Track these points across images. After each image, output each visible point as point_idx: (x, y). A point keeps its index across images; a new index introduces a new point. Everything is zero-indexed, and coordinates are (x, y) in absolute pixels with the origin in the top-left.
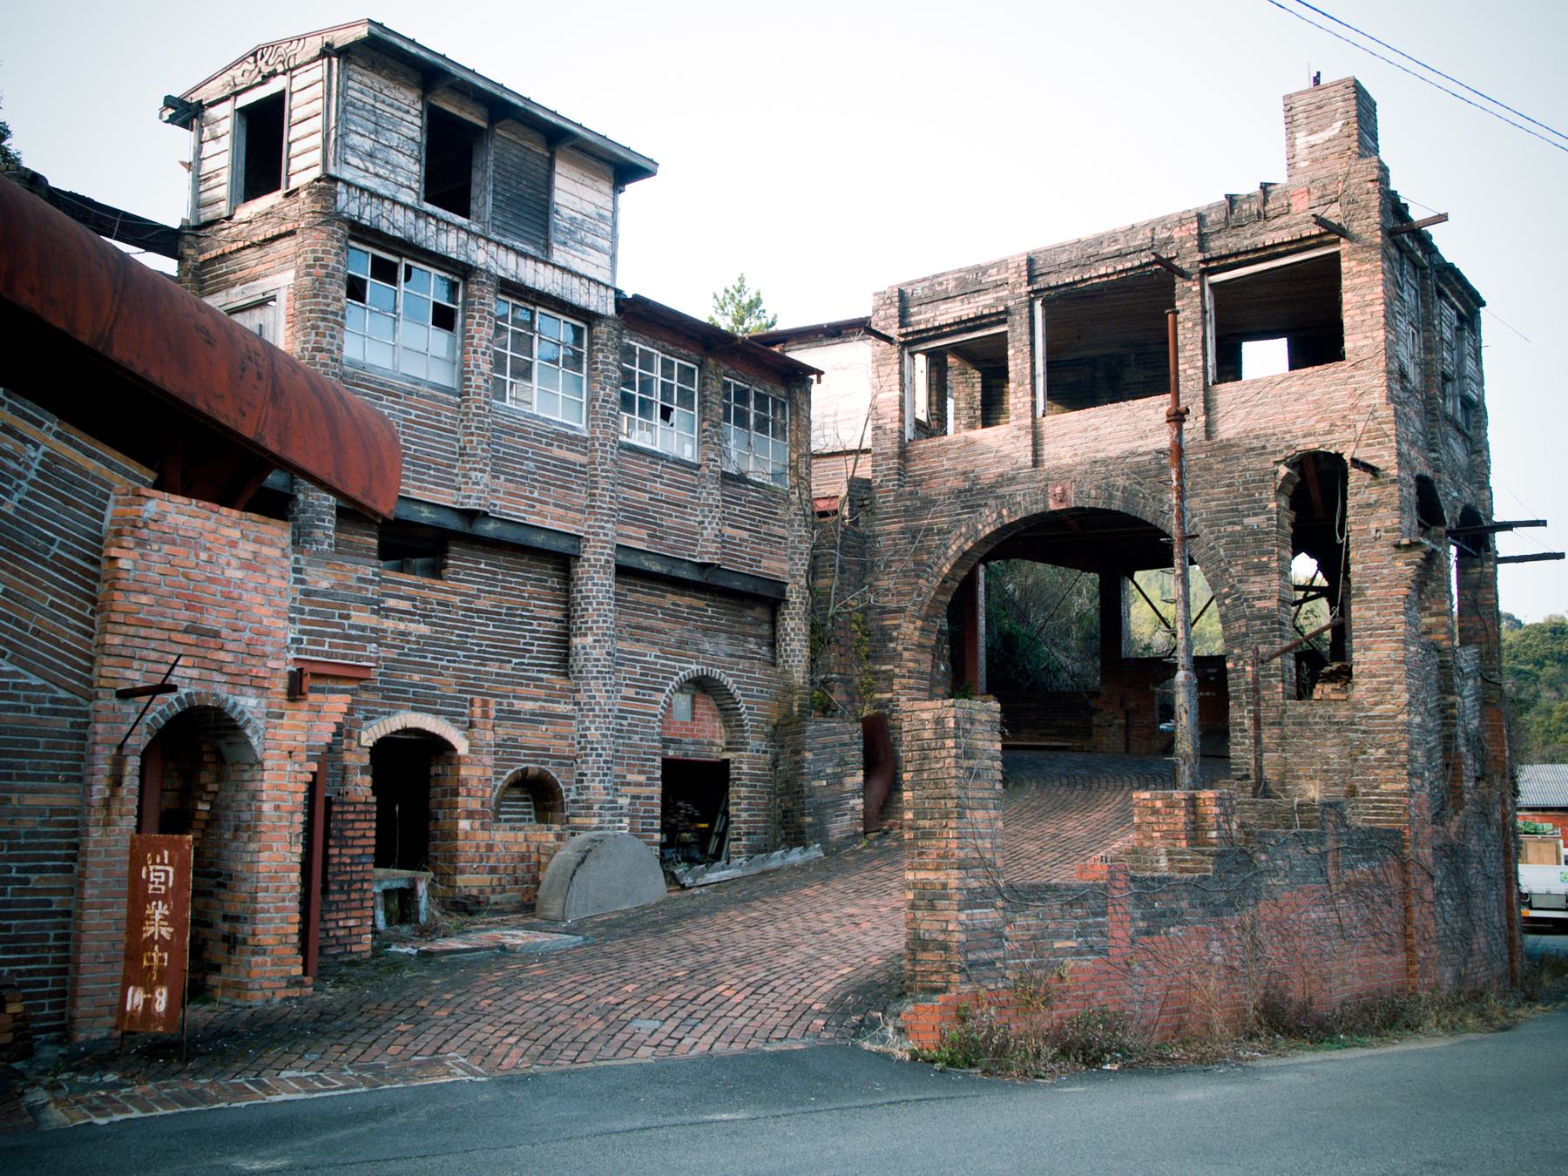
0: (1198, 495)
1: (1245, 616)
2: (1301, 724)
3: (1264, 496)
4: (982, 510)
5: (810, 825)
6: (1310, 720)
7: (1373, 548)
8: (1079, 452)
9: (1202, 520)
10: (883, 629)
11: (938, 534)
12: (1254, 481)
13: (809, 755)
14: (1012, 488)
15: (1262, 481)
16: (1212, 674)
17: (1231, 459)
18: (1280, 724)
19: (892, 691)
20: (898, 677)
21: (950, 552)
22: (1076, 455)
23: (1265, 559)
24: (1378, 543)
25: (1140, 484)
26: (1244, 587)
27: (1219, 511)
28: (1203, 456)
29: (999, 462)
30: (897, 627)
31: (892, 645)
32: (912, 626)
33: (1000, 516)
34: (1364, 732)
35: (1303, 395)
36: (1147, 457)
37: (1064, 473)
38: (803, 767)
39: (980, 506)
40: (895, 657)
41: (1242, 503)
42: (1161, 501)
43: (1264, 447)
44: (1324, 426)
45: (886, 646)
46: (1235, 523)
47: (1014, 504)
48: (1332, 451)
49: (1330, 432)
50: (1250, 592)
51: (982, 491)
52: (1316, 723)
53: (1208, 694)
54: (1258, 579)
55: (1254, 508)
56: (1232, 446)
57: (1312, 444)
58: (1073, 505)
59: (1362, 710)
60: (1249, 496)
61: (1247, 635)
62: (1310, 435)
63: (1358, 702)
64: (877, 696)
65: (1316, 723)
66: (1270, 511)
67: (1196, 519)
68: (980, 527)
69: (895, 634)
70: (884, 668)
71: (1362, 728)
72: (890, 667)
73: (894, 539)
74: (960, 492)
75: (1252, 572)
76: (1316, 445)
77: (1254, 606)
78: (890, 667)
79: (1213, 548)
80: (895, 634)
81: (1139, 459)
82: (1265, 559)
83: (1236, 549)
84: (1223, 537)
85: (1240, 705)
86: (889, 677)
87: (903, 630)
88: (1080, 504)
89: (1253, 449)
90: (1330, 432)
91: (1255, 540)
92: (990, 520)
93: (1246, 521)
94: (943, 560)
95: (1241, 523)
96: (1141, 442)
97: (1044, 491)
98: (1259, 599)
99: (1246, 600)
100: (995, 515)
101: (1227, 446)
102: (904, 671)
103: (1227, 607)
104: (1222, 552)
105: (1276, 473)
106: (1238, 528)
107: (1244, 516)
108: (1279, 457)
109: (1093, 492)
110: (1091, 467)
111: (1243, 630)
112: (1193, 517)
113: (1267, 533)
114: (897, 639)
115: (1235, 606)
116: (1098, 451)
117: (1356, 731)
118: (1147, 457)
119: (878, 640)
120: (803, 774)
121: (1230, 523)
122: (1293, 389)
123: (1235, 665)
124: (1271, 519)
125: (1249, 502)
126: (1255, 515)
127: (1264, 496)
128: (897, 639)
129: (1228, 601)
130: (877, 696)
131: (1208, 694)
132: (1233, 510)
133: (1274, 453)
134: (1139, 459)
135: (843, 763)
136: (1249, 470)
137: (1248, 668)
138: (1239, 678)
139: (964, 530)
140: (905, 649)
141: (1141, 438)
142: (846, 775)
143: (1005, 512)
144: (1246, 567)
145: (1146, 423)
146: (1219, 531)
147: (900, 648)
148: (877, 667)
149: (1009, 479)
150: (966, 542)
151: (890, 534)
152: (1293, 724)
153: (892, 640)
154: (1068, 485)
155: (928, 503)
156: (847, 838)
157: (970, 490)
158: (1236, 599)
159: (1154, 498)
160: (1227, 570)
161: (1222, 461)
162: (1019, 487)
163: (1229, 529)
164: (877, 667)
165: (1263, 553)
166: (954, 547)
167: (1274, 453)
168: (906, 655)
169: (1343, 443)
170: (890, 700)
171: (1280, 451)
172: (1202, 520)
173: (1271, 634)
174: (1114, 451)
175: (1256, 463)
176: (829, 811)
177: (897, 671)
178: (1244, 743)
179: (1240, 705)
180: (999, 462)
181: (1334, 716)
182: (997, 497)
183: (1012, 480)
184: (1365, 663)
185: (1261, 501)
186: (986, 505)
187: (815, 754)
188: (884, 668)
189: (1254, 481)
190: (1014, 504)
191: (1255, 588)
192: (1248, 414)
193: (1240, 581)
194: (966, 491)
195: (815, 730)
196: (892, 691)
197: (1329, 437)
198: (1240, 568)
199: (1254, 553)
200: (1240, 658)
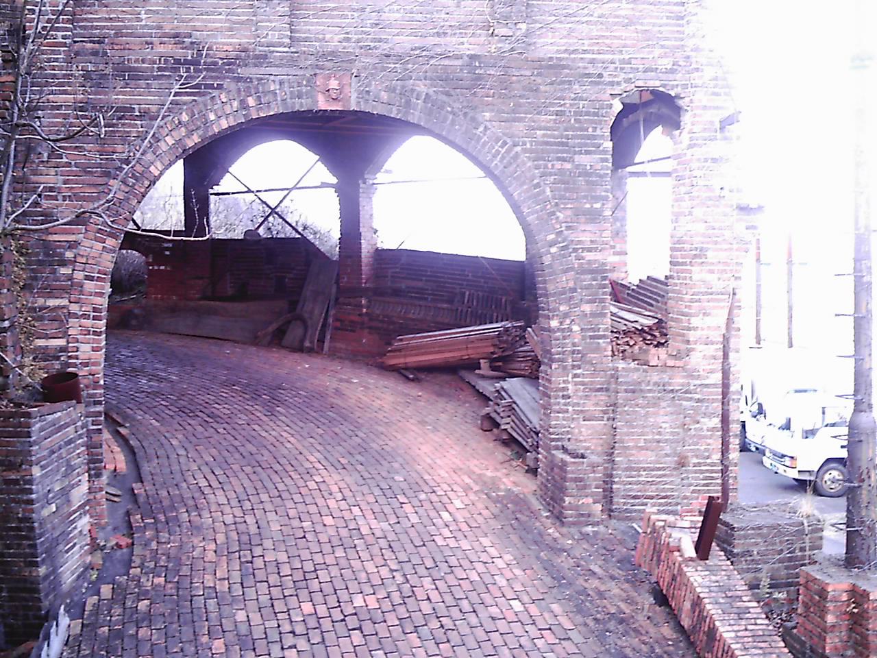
0: (520, 120)
1: (572, 269)
2: (634, 391)
3: (598, 132)
4: (215, 93)
5: (46, 577)
6: (643, 387)
7: (718, 206)
8: (354, 37)
9: (525, 151)
10: (47, 245)
11: (140, 117)
12: (588, 114)
13: (36, 472)
14: (263, 70)
15: (596, 114)
16: (167, 249)
17: (563, 83)
18: (607, 390)
19: (65, 335)
20: (76, 316)
21: (163, 147)
22: (348, 40)
23: (598, 205)
24: (723, 202)
25: (448, 94)
26: (573, 236)
27: (547, 143)
28: (528, 73)
29: (231, 29)
30: (73, 245)
31: (63, 270)
32: (99, 246)
33: (244, 105)
34: (698, 401)
35: (631, 23)
36: (459, 62)
37: (336, 60)
38: (31, 492)
39: (211, 86)
40: (71, 288)
41: (573, 137)
42: (473, 119)
43: (600, 75)
44: (666, 63)
45: (54, 272)
46: (564, 160)
47: (265, 93)
48: (673, 93)
49: (672, 71)
50: (580, 242)
51: (212, 67)
52: (650, 391)
53: (162, 268)
54: (589, 227)
55: (586, 145)
56: (564, 67)
57: (654, 84)
58: (353, 107)
59: (698, 377)
60: (581, 129)
61: (574, 290)
62: (651, 70)
63: (695, 370)
64: (41, 343)
65: (650, 391)
66: (605, 152)
67: (518, 149)
68: (212, 117)
69: (69, 255)
70: (52, 303)
71: (697, 396)
72: (64, 302)
73: (66, 117)
74: (178, 62)
75: (582, 219)
76: (657, 83)
77: (583, 258)
78: (64, 302)
79: (538, 185)
80: (69, 255)
81: (446, 62)
82: (598, 205)
83: (566, 190)
84: (551, 174)
85: (565, 368)
86: (60, 319)
87: (82, 250)
88: (364, 108)
89: (588, 75)
90: (672, 71)
91: (588, 182)
92: (228, 109)
93: (577, 158)
94: (149, 156)
95: (571, 160)
96: (437, 40)
97: (310, 81)
98: (590, 250)
99: (575, 250)
100: (235, 104)
101: (553, 67)
102: (87, 309)
103: (553, 257)
104: (548, 193)
105: (611, 106)
106: (568, 166)
107: (575, 153)
108: (617, 90)
109: (384, 96)
110: (381, 62)
111: (571, 284)
112: (515, 145)
113: (601, 176)
114: (73, 262)
115: (564, 256)
116: (380, 41)
117: (691, 399)
118: (459, 62)
119: (40, 263)
120: (31, 502)
121: (559, 159)
122: (622, 13)
123: (561, 323)
124: (606, 160)
125: (581, 137)
126: (587, 153)
127: (598, 132)
128: (73, 262)
129: (553, 250)
130: (41, 343)
131: (162, 268)
132: (562, 144)
133: (612, 84)
134: (446, 62)
135: (70, 468)
136: (581, 99)
137: (576, 328)
138: (564, 338)
139: (185, 118)
140: (88, 278)
141: (438, 34)
142: (73, 487)
143: (251, 101)
144: (578, 213)
145: (443, 16)
146: (546, 167)
147: (79, 276)
148: (41, 302)
149: (257, 57)
150: (190, 133)
151: (59, 108)
152: (626, 391)
153: (64, 263)
154: (346, 80)
155: (128, 74)
156: (79, 577)
157: (195, 62)
158: (563, 248)
159: (465, 114)
160: (553, 213)
161: (552, 84)
162: (274, 71)
163: (558, 165)
164: (41, 302)
165: (597, 199)
166: (170, 140)
167: (612, 84)
168: (89, 286)
169: (685, 86)
170: (63, 349)
171: (618, 83)
172: (525, 151)
173: (601, 291)
174: (404, 43)
175: (591, 92)
176: (60, 547)
177: (74, 308)
178: (567, 411)
179: (565, 368)
180: (231, 29)
181: (670, 384)
182: (239, 79)
183: (261, 59)
184: (702, 329)
185: (594, 137)
186: (220, 87)
187: (43, 468)
188: (52, 303)
189: (588, 114)
190: (265, 93)
191: (586, 238)
192: (571, 30)
193: (568, 228)
194: (186, 62)
195: (41, 429)
196: (65, 335)
197: (671, 76)
198: (569, 213)
199: (585, 197)
200: (566, 315)
